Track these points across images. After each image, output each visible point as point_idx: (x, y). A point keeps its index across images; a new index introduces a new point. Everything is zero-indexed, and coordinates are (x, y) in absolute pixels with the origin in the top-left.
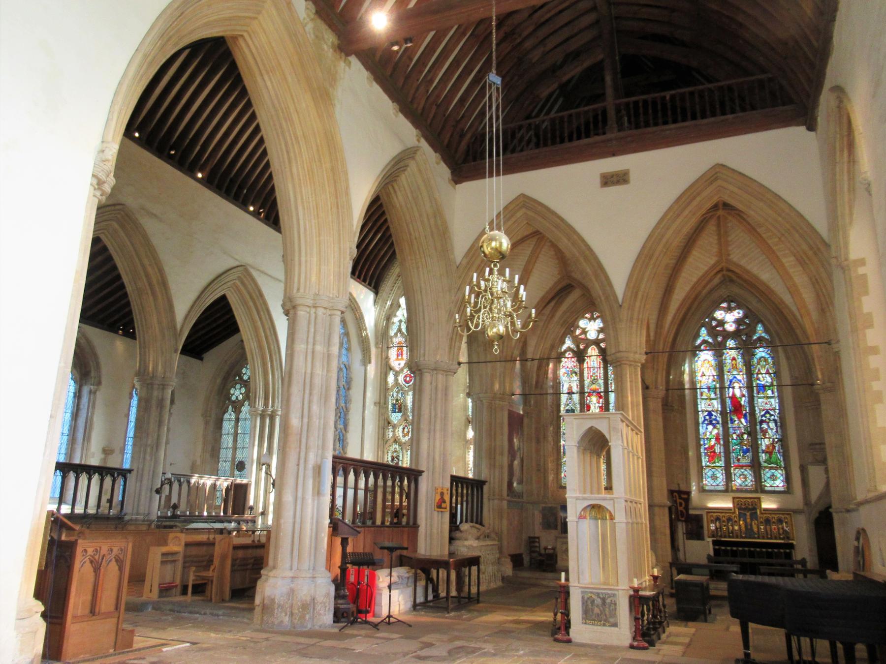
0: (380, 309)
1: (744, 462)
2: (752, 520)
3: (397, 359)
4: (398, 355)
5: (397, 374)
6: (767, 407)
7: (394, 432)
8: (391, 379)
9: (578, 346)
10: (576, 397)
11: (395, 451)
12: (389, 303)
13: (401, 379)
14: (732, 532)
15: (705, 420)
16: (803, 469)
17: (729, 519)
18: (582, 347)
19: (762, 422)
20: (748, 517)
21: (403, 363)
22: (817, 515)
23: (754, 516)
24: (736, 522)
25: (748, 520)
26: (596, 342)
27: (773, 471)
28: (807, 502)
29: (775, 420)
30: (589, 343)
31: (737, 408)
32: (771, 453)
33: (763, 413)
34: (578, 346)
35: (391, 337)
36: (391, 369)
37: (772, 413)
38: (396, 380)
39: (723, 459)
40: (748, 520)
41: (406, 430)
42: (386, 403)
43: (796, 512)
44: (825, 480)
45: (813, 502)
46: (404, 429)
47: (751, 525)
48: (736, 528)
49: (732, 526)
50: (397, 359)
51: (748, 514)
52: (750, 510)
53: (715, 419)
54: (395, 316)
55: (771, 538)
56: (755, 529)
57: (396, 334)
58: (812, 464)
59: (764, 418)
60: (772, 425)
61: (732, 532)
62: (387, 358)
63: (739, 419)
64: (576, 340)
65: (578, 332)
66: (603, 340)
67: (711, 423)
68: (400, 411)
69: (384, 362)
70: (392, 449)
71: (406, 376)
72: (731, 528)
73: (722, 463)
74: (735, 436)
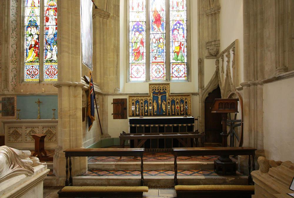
1: (159, 60)
2: (162, 102)
6: (178, 19)
10: (37, 11)
14: (147, 112)
15: (134, 28)
16: (201, 62)
17: (146, 102)
19: (174, 30)
20: (160, 99)
22: (207, 95)
23: (164, 99)
24: (150, 103)
25: (160, 102)
27: (178, 66)
28: (201, 86)
29: (183, 28)
31: (158, 20)
32: (178, 53)
33: (175, 23)
37: (181, 23)
39: (145, 57)
40: (160, 102)
43: (194, 94)
44: (215, 69)
45: (205, 87)
47: (161, 105)
48: (150, 108)
49: (148, 107)
51: (160, 97)
52: (161, 93)
53: (141, 28)
55: (174, 115)
56: (164, 109)
58: (207, 57)
59: (175, 27)
60: (181, 31)
61: (147, 112)
63: (158, 27)
67: (138, 31)
72: (146, 108)
73: (144, 61)
74: (154, 40)
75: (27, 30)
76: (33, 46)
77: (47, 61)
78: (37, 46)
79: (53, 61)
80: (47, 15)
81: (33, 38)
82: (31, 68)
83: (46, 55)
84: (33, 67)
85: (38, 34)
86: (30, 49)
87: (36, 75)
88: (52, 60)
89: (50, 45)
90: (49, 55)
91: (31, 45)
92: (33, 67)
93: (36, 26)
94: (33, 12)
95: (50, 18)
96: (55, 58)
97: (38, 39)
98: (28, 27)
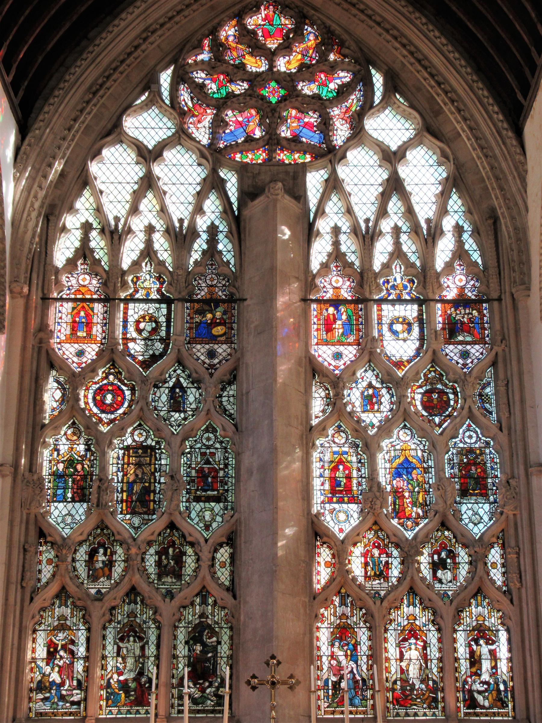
0: (32, 179)
3: (73, 338)
4: (75, 326)
5: (72, 382)
7: (58, 561)
8: (52, 396)
11: (62, 627)
12: (58, 166)
13: (86, 397)
21: (91, 351)
35: (57, 271)
36: (52, 366)
38: (69, 398)
41: (101, 557)
42: (33, 465)
46: (92, 554)
50: (73, 338)
54: (71, 209)
57: (71, 263)
62: (44, 330)
68: (81, 496)
69: (31, 342)
70: (50, 621)
71: (101, 390)
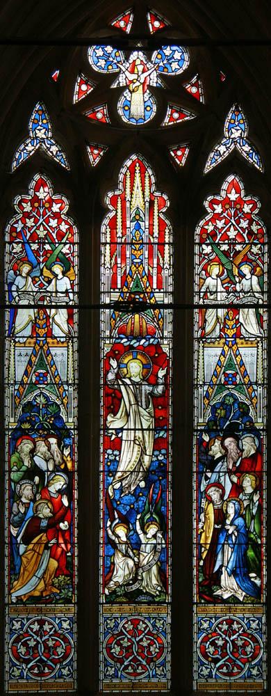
9: (77, 156)
18: (94, 157)
26: (149, 142)
30: (123, 139)
34: (77, 156)
64: (72, 128)
65: (82, 90)
66: (179, 134)
75: (15, 449)
76: (44, 523)
77: (112, 598)
78: (63, 526)
79: (143, 598)
80: (111, 376)
81: (42, 488)
82: (36, 627)
83: (110, 569)
84: (41, 623)
85: (66, 471)
86: (27, 540)
87: (55, 662)
88: (139, 592)
89: (125, 520)
90: (122, 568)
91: (36, 519)
92: (41, 623)
93: (61, 433)
94: (41, 364)
95: (127, 396)
96: (152, 581)
97: (67, 491)
98: (20, 434)
